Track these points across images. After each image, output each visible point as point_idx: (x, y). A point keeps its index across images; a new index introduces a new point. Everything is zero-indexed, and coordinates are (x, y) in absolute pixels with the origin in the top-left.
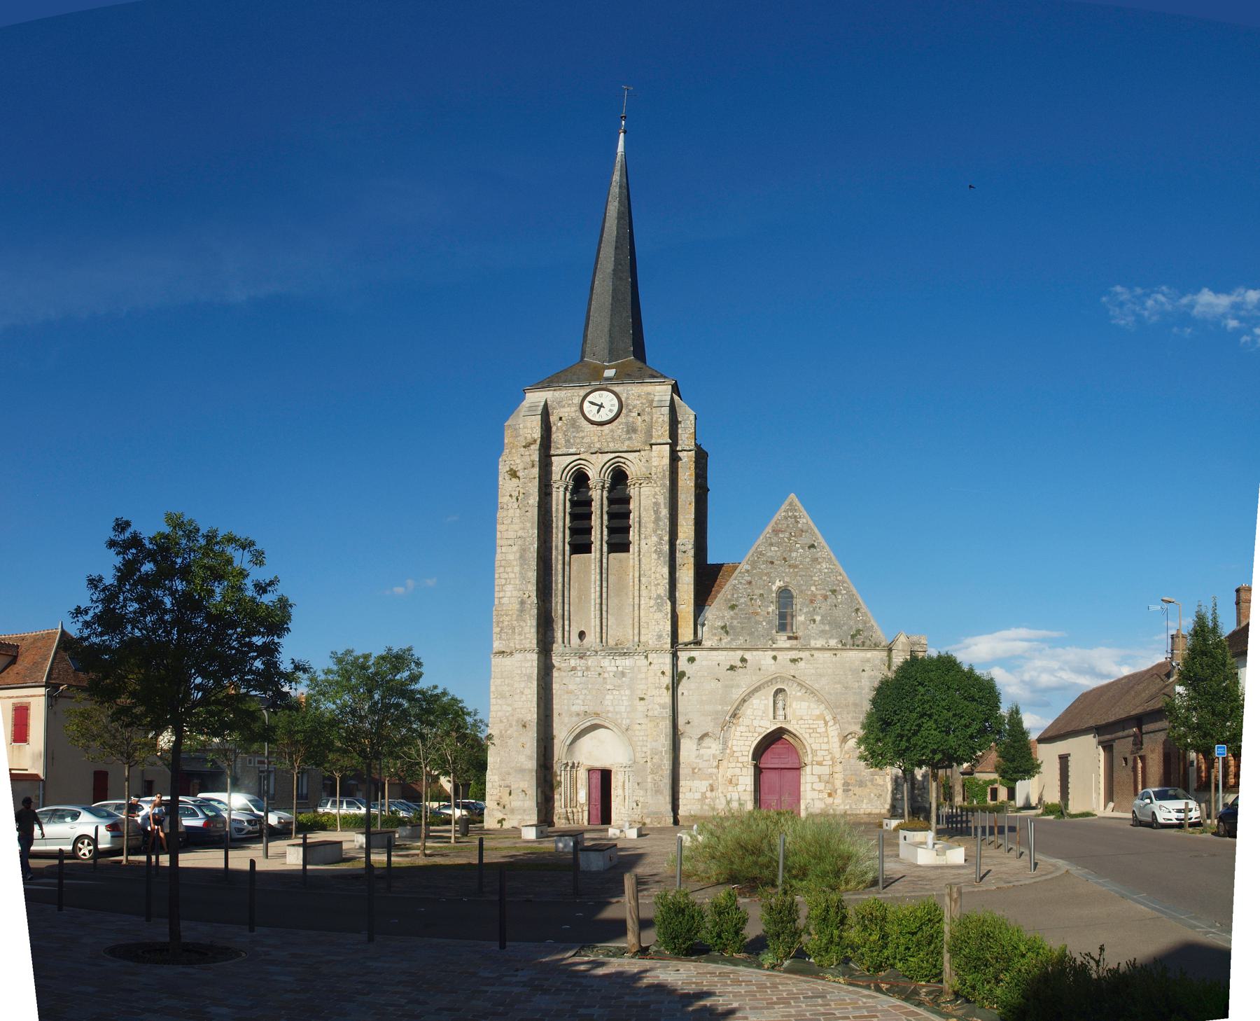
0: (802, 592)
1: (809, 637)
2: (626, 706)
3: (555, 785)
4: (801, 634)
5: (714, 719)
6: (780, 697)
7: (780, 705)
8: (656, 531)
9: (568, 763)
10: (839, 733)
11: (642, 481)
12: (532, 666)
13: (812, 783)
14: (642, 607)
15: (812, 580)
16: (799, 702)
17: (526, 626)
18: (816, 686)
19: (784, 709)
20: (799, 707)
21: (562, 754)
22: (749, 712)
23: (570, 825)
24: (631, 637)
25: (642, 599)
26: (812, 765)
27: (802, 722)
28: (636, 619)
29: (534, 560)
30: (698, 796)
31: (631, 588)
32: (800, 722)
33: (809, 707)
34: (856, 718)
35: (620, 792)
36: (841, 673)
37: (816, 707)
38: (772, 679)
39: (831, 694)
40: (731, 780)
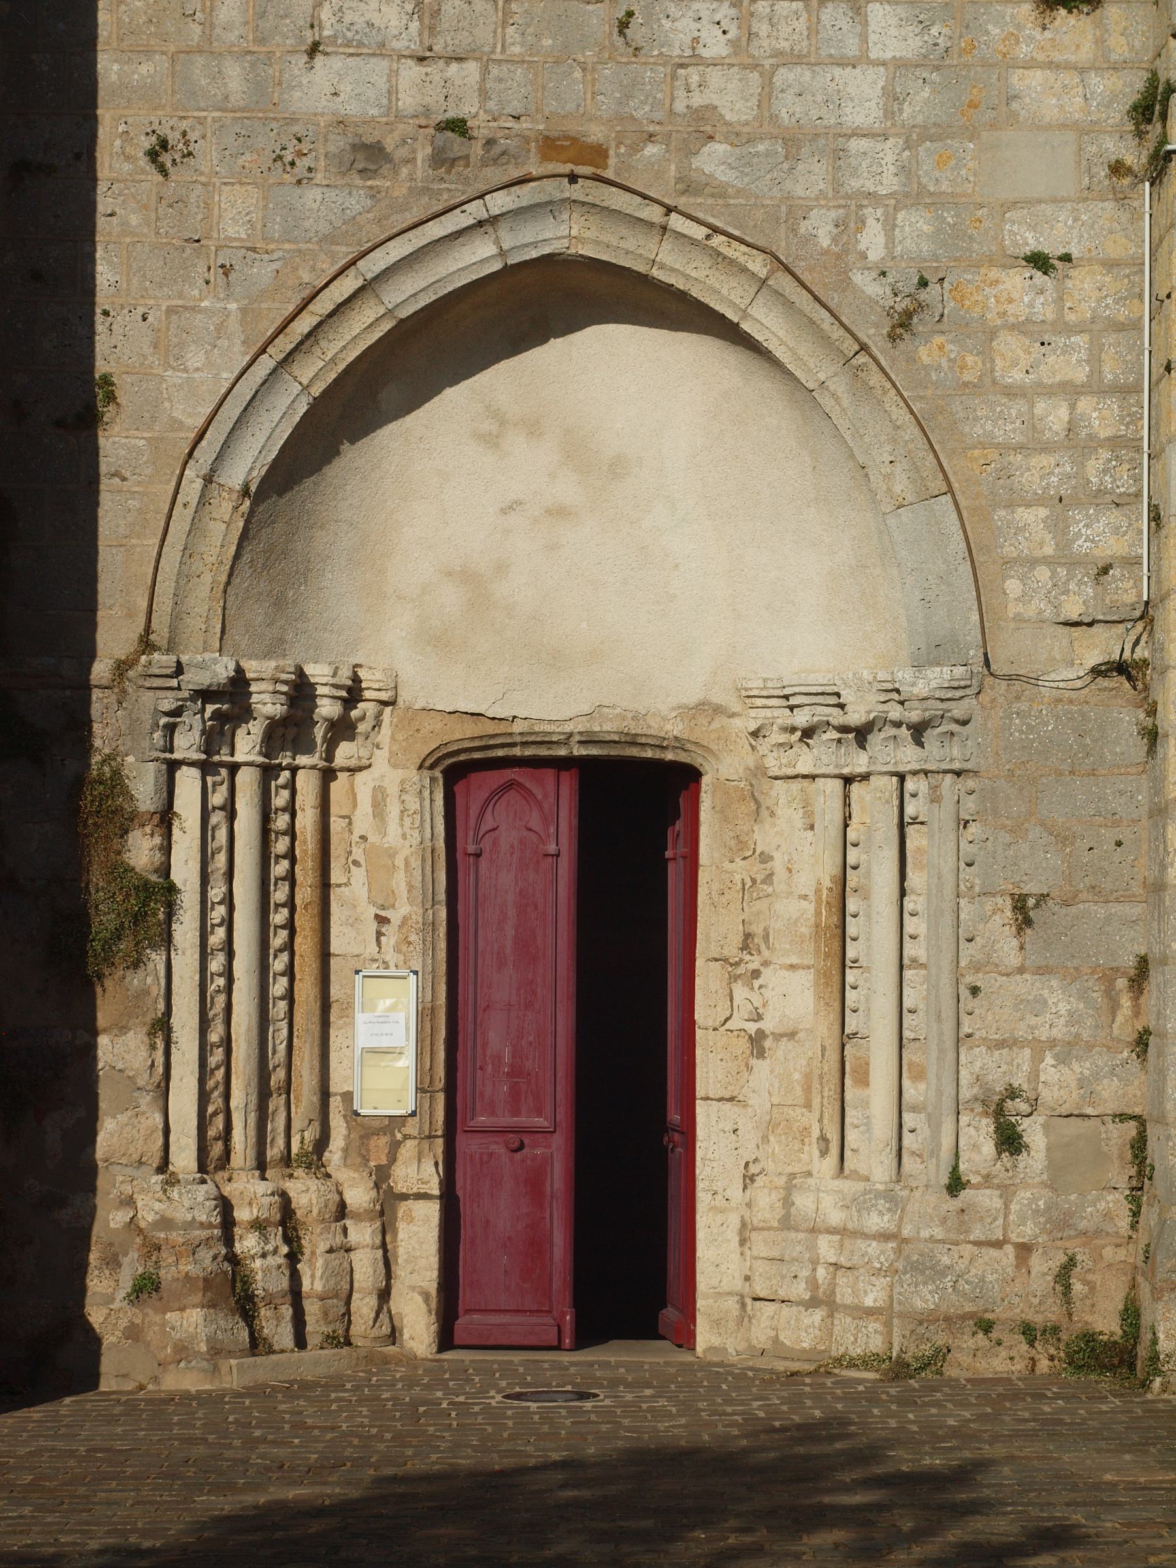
2: (900, 65)
3: (104, 920)
9: (239, 683)
21: (184, 577)
23: (262, 1369)
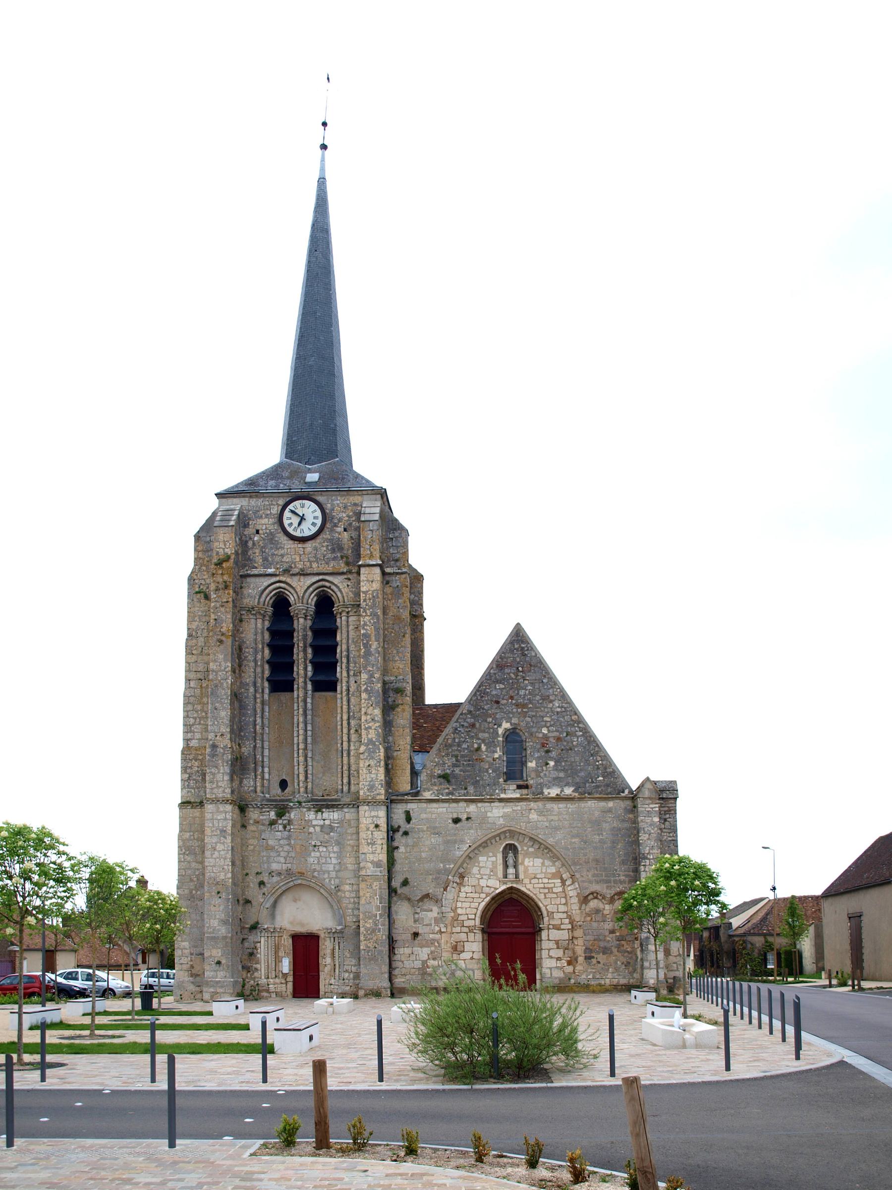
0: (532, 735)
1: (542, 786)
4: (531, 782)
5: (437, 878)
6: (511, 855)
7: (511, 861)
8: (366, 666)
11: (350, 609)
12: (226, 819)
14: (352, 753)
15: (543, 721)
16: (532, 859)
17: (219, 772)
18: (551, 841)
19: (515, 867)
22: (475, 870)
24: (340, 787)
25: (352, 744)
26: (549, 929)
27: (536, 881)
28: (345, 768)
29: (227, 698)
30: (418, 964)
31: (339, 733)
32: (533, 881)
33: (543, 864)
34: (597, 875)
35: (328, 960)
36: (579, 825)
37: (551, 864)
38: (501, 833)
39: (569, 850)
40: (456, 946)
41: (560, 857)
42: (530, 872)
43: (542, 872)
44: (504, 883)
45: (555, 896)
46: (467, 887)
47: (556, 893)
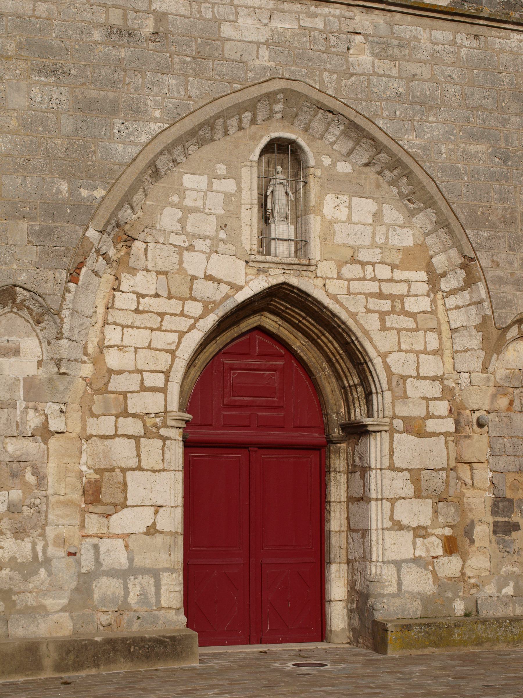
10: (484, 318)
13: (393, 501)
16: (345, 198)
20: (342, 214)
26: (392, 431)
27: (355, 271)
32: (349, 271)
33: (377, 217)
36: (488, 103)
37: (401, 220)
38: (259, 99)
41: (438, 197)
42: (339, 239)
43: (373, 245)
44: (260, 271)
45: (409, 323)
46: (140, 275)
47: (412, 315)
